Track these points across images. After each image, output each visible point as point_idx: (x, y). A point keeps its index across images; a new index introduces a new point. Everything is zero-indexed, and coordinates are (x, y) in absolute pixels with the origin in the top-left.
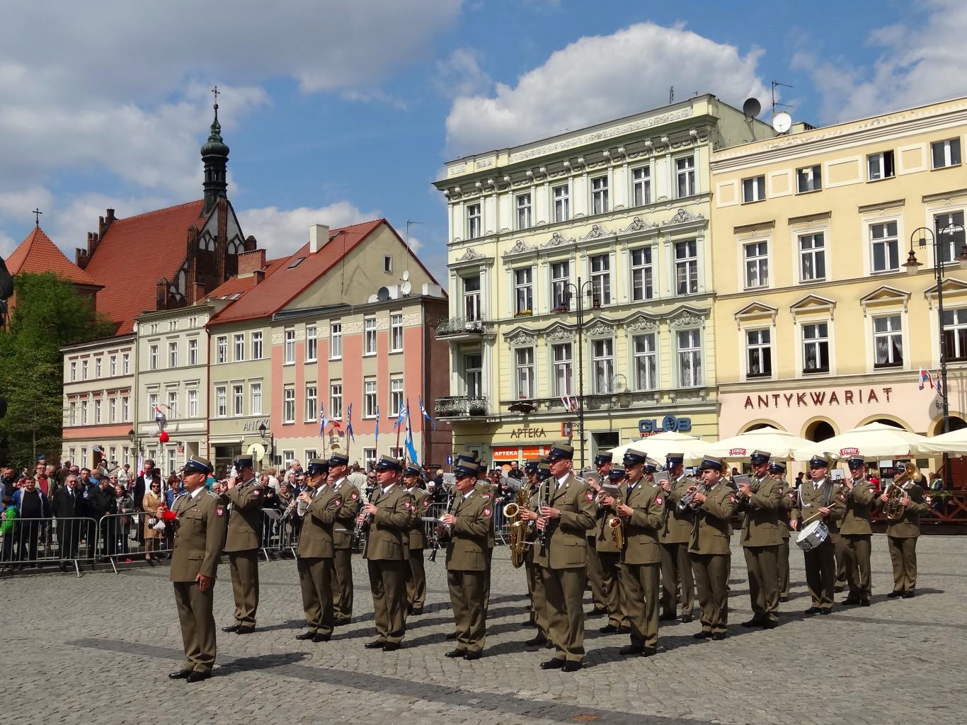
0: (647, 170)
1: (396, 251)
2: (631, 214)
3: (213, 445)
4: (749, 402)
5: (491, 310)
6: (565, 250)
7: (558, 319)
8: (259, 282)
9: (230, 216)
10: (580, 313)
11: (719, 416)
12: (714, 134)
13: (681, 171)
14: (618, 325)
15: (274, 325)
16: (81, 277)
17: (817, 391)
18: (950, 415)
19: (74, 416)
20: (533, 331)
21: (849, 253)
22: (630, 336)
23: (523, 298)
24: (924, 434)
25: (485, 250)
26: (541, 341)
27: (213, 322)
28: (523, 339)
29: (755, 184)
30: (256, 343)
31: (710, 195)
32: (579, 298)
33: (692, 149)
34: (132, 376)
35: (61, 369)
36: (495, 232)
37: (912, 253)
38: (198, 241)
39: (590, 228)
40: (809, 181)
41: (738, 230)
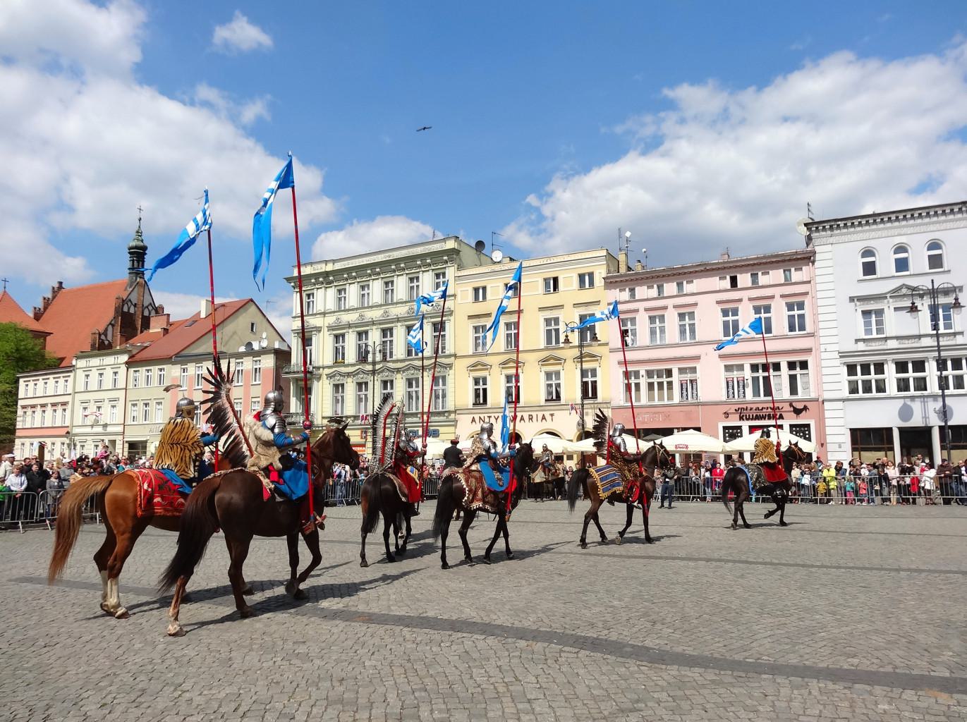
0: (418, 278)
1: (258, 319)
2: (407, 304)
3: (127, 442)
4: (473, 420)
5: (318, 362)
6: (366, 324)
7: (360, 367)
8: (164, 335)
9: (147, 291)
10: (374, 363)
11: (456, 428)
12: (458, 260)
13: (438, 281)
14: (397, 372)
15: (174, 363)
16: (36, 326)
18: (586, 430)
19: (24, 421)
20: (345, 373)
21: (533, 335)
22: (404, 379)
23: (339, 353)
24: (571, 441)
26: (350, 380)
27: (130, 360)
28: (338, 378)
29: (481, 291)
30: (161, 375)
31: (454, 295)
32: (374, 354)
33: (445, 268)
34: (70, 394)
35: (17, 388)
36: (323, 311)
37: (567, 336)
38: (123, 305)
39: (382, 312)
41: (470, 317)
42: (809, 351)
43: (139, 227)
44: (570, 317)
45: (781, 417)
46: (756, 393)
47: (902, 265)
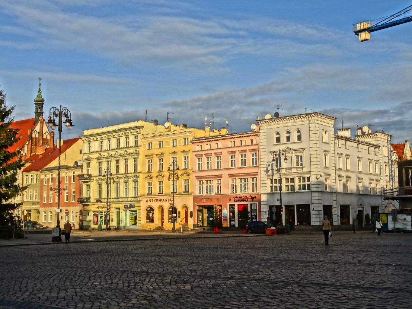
4: (147, 201)
17: (160, 198)
40: (161, 144)
41: (146, 156)
42: (256, 174)
43: (40, 89)
45: (247, 201)
47: (288, 139)
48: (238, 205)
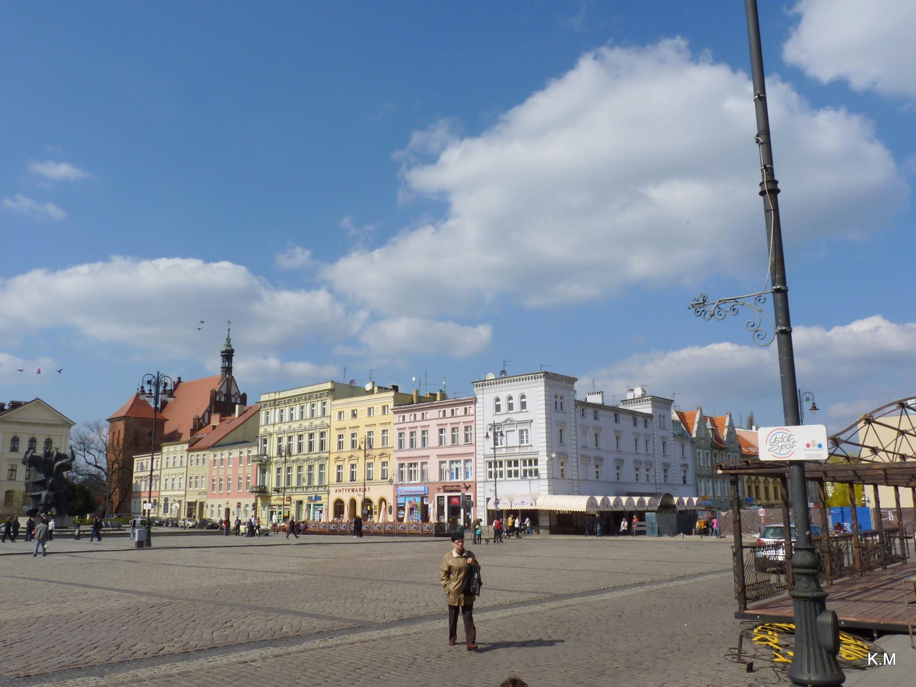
25: (270, 429)
41: (337, 429)
44: (361, 435)
46: (451, 477)
47: (511, 407)
48: (449, 498)
